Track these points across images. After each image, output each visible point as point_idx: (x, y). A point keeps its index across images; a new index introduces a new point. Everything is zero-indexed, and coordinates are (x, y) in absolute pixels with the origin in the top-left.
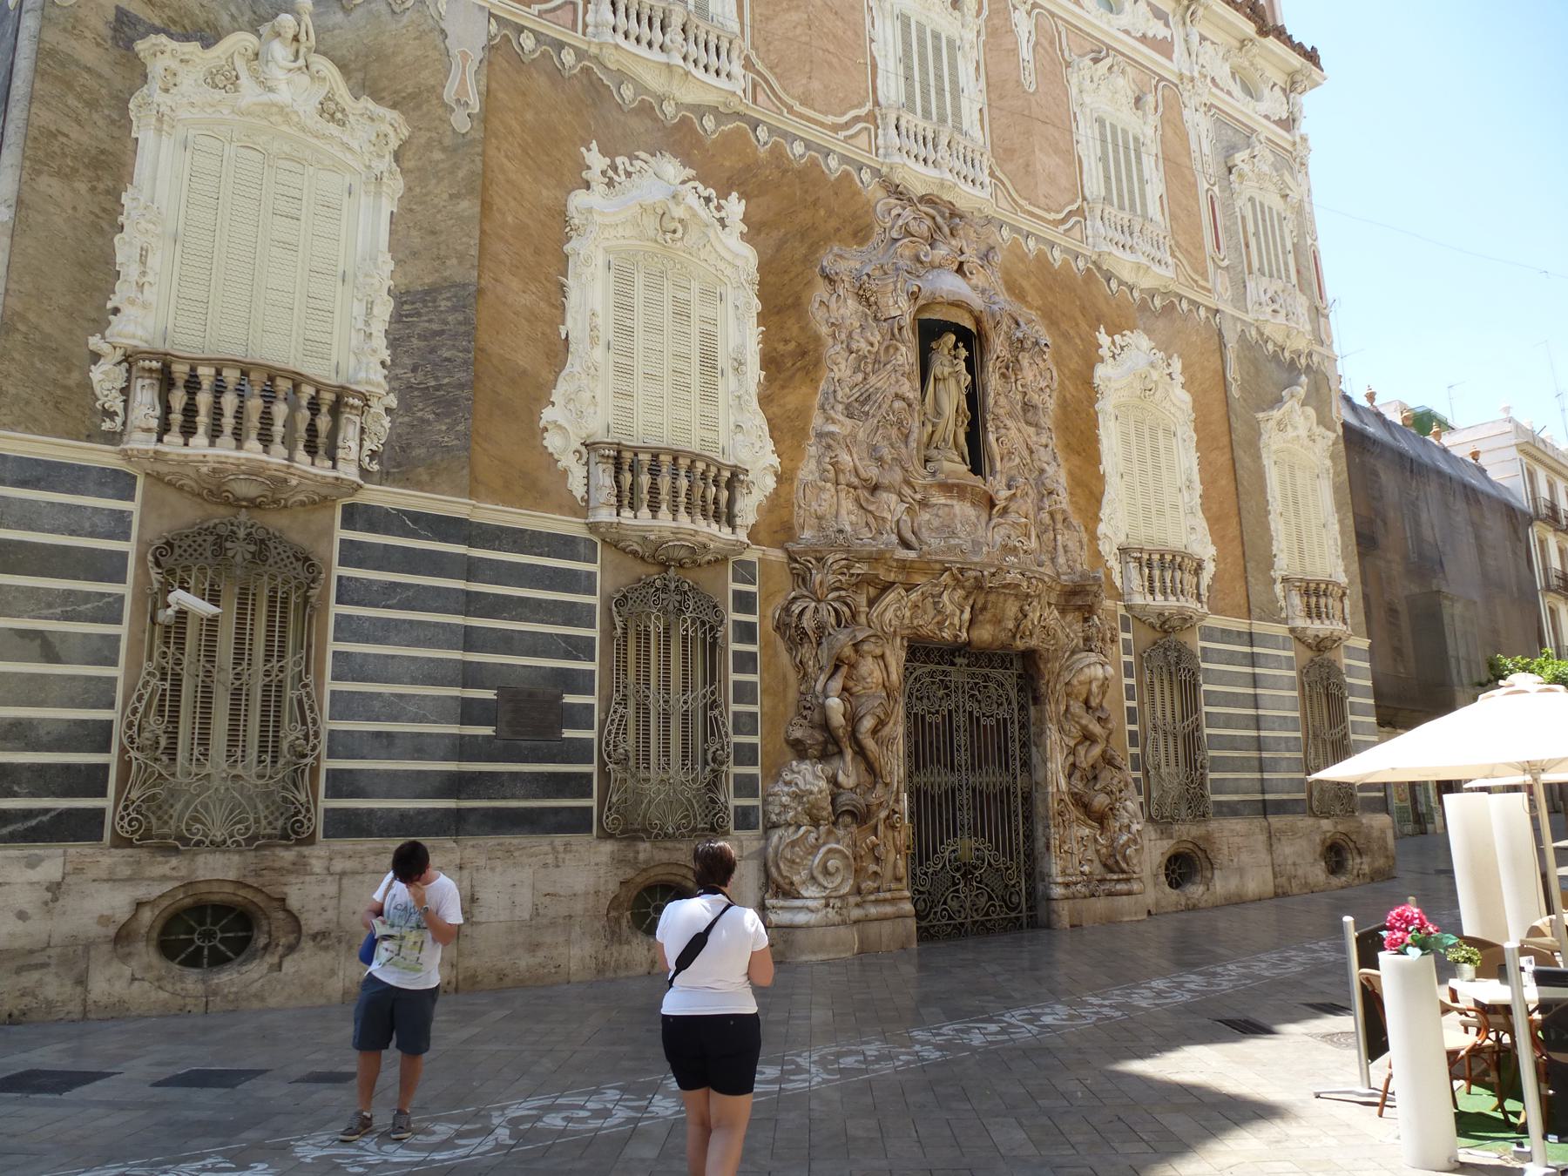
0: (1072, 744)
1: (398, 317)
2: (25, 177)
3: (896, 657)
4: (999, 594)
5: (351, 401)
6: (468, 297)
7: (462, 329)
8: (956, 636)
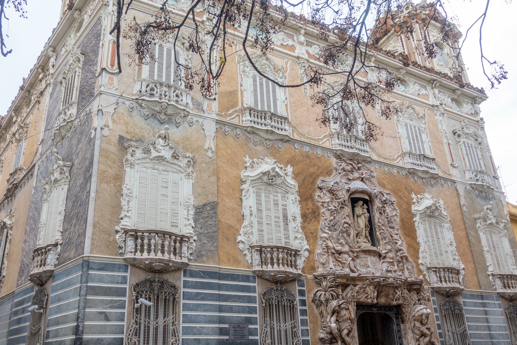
1: (196, 213)
2: (98, 184)
3: (352, 308)
4: (386, 286)
5: (185, 239)
6: (214, 206)
7: (214, 215)
8: (373, 301)
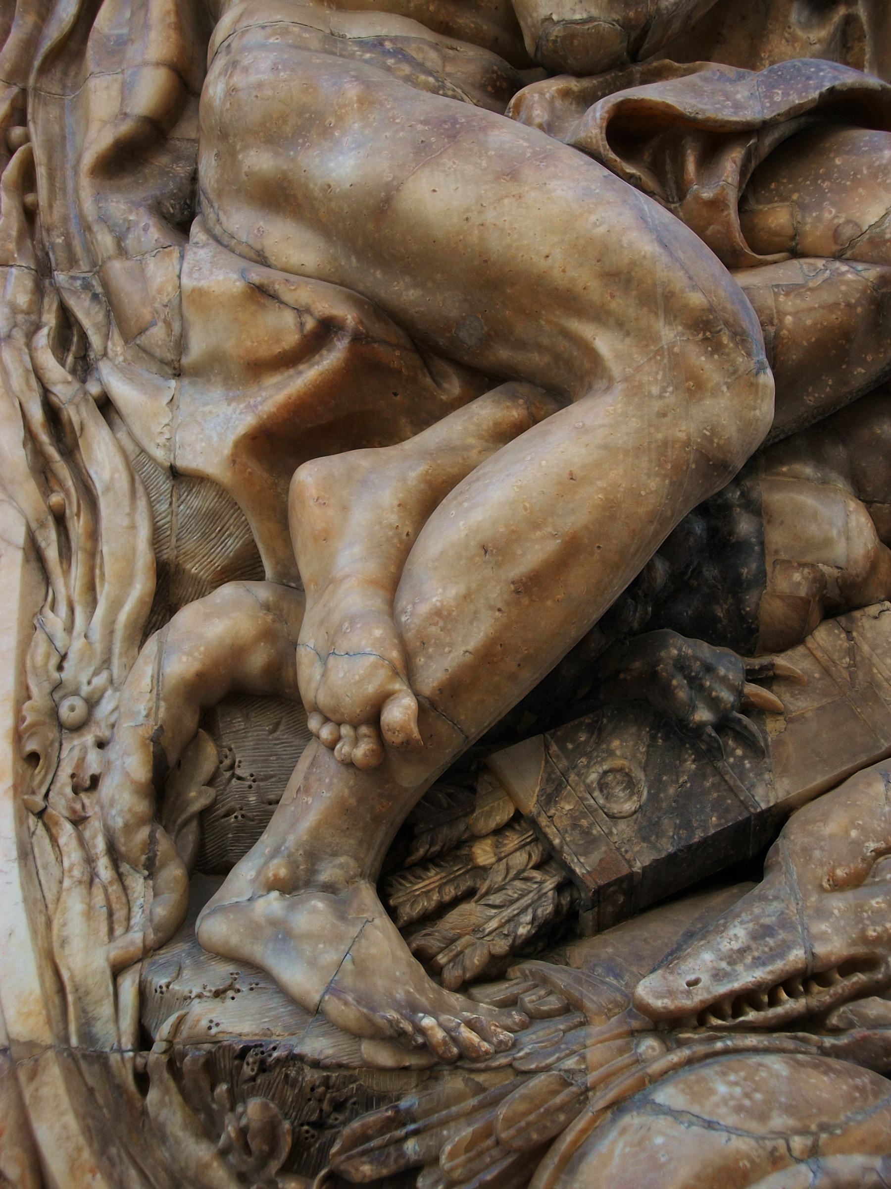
0: (211, 429)
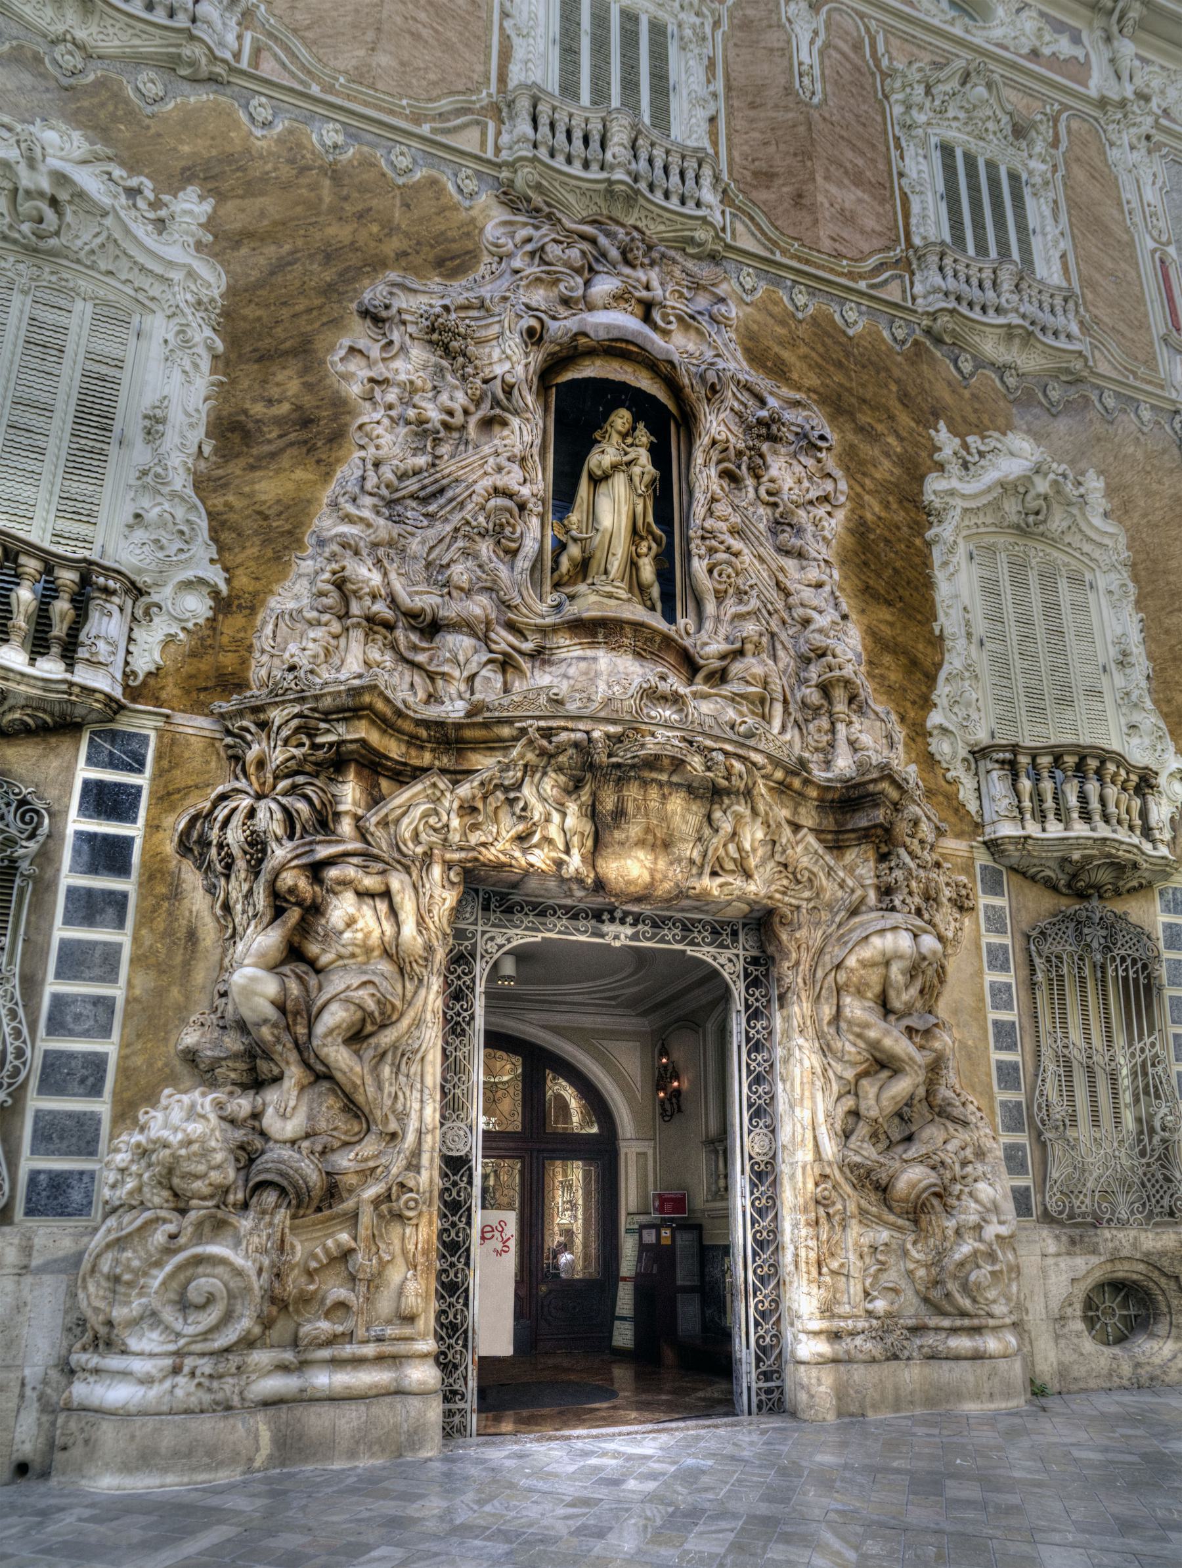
4: (645, 783)
8: (559, 864)
